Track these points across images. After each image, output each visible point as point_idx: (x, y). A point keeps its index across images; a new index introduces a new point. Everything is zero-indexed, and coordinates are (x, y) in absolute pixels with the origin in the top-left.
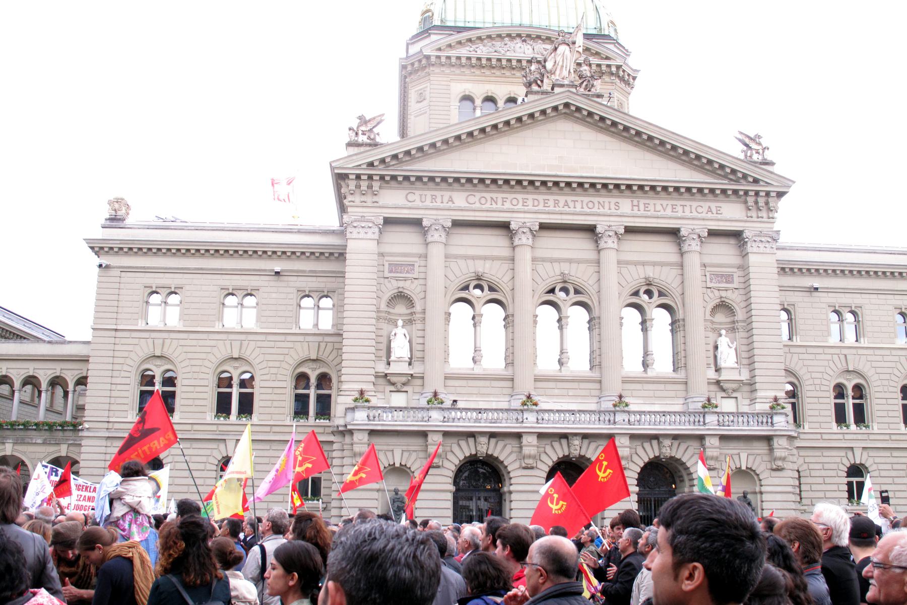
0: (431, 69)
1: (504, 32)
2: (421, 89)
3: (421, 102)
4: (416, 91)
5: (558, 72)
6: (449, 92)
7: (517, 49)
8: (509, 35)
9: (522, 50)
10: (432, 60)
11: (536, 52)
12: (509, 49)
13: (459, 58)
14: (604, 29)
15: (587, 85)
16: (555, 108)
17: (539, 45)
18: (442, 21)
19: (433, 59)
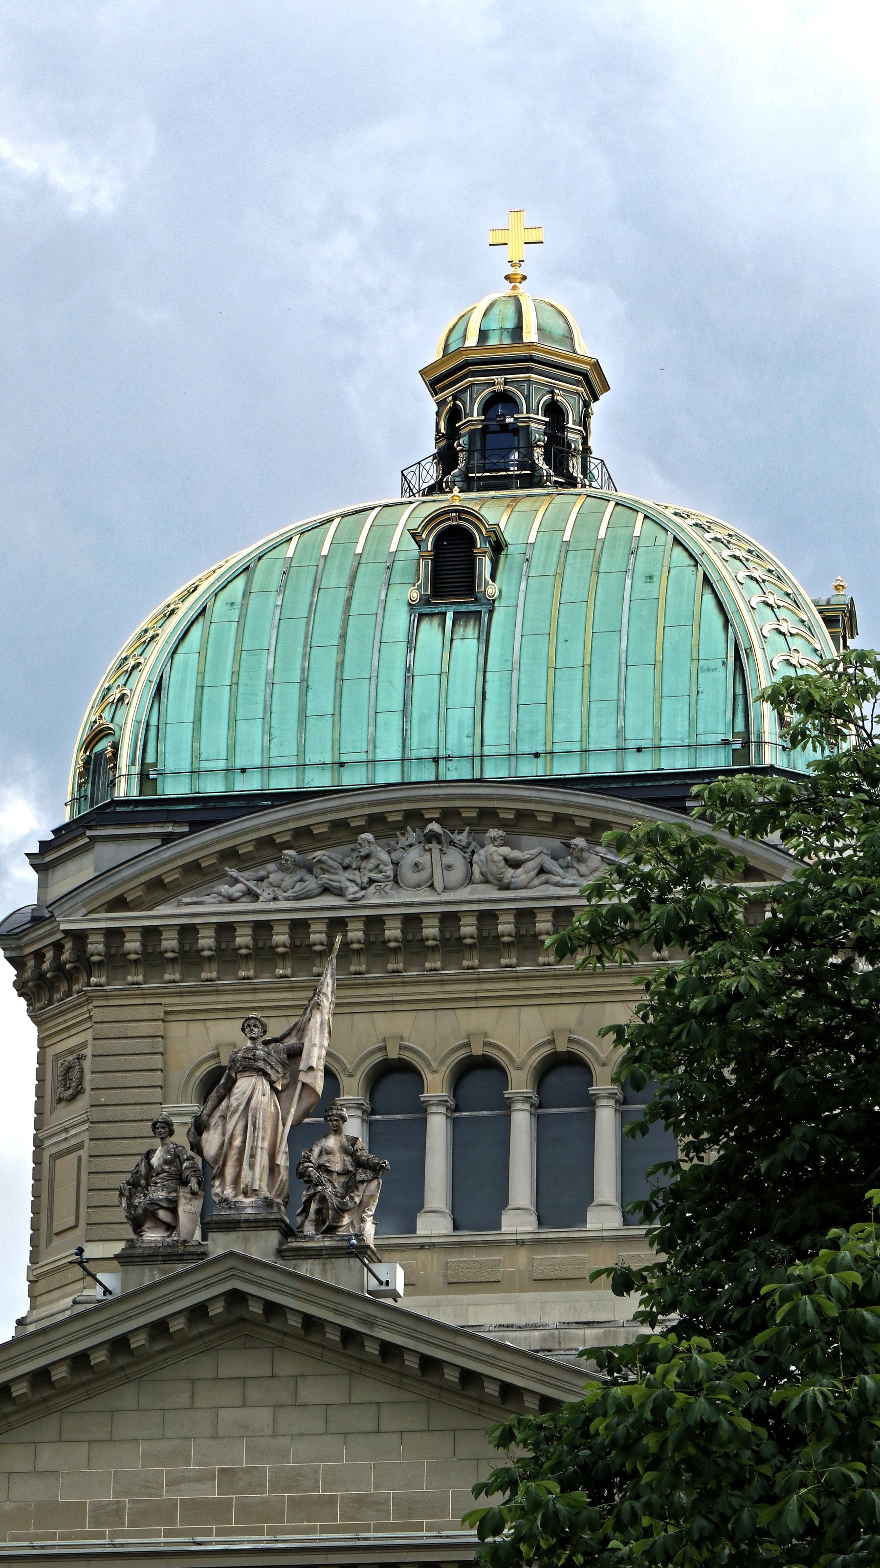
0: (93, 980)
1: (357, 815)
2: (71, 1051)
3: (72, 1099)
4: (57, 1057)
5: (230, 1172)
6: (157, 1061)
7: (408, 875)
8: (376, 822)
9: (425, 874)
10: (91, 948)
11: (477, 875)
12: (373, 875)
13: (188, 932)
14: (760, 744)
15: (318, 1212)
16: (198, 1312)
17: (491, 848)
18: (144, 777)
19: (96, 946)
